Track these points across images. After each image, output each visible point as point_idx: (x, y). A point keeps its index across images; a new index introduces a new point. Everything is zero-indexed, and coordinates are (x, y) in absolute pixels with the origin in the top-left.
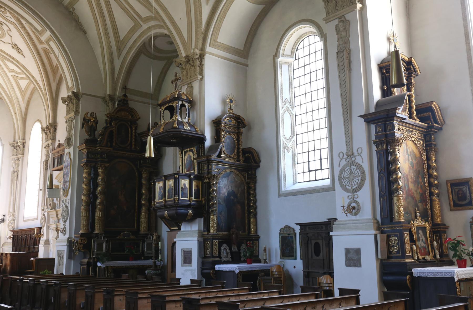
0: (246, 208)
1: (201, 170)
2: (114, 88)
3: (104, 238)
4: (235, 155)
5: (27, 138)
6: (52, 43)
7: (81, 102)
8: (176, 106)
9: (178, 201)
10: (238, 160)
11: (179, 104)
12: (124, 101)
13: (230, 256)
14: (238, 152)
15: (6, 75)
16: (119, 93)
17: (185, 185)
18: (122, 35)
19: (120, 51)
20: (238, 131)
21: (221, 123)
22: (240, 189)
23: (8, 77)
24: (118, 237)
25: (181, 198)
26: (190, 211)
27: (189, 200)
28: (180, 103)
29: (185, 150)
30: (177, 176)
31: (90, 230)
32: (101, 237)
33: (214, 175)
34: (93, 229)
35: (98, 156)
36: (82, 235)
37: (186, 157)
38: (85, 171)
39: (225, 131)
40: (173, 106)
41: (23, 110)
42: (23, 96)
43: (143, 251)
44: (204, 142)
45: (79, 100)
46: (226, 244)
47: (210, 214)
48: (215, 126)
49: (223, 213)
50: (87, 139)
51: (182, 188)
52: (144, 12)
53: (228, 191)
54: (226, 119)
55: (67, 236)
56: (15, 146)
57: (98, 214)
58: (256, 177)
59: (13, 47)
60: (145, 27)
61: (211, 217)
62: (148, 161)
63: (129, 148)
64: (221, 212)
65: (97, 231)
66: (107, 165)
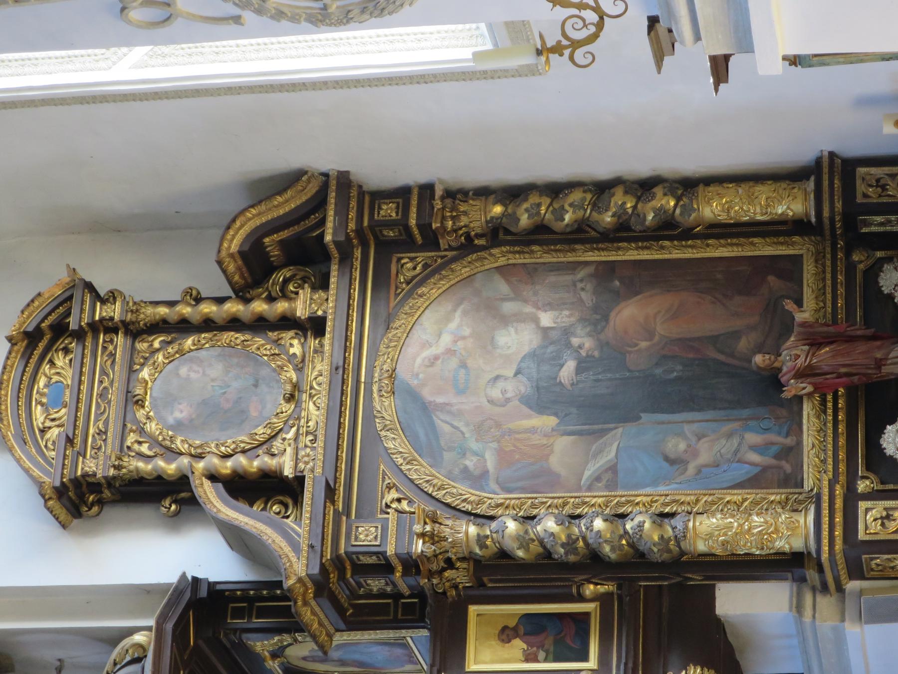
0: (633, 254)
14: (260, 325)
20: (115, 330)
21: (76, 482)
22: (509, 307)
33: (422, 535)
39: (123, 440)
44: (211, 585)
46: (881, 431)
47: (683, 553)
48: (95, 509)
49: (677, 446)
53: (526, 410)
54: (43, 431)
58: (427, 189)
61: (701, 547)
64: (667, 459)
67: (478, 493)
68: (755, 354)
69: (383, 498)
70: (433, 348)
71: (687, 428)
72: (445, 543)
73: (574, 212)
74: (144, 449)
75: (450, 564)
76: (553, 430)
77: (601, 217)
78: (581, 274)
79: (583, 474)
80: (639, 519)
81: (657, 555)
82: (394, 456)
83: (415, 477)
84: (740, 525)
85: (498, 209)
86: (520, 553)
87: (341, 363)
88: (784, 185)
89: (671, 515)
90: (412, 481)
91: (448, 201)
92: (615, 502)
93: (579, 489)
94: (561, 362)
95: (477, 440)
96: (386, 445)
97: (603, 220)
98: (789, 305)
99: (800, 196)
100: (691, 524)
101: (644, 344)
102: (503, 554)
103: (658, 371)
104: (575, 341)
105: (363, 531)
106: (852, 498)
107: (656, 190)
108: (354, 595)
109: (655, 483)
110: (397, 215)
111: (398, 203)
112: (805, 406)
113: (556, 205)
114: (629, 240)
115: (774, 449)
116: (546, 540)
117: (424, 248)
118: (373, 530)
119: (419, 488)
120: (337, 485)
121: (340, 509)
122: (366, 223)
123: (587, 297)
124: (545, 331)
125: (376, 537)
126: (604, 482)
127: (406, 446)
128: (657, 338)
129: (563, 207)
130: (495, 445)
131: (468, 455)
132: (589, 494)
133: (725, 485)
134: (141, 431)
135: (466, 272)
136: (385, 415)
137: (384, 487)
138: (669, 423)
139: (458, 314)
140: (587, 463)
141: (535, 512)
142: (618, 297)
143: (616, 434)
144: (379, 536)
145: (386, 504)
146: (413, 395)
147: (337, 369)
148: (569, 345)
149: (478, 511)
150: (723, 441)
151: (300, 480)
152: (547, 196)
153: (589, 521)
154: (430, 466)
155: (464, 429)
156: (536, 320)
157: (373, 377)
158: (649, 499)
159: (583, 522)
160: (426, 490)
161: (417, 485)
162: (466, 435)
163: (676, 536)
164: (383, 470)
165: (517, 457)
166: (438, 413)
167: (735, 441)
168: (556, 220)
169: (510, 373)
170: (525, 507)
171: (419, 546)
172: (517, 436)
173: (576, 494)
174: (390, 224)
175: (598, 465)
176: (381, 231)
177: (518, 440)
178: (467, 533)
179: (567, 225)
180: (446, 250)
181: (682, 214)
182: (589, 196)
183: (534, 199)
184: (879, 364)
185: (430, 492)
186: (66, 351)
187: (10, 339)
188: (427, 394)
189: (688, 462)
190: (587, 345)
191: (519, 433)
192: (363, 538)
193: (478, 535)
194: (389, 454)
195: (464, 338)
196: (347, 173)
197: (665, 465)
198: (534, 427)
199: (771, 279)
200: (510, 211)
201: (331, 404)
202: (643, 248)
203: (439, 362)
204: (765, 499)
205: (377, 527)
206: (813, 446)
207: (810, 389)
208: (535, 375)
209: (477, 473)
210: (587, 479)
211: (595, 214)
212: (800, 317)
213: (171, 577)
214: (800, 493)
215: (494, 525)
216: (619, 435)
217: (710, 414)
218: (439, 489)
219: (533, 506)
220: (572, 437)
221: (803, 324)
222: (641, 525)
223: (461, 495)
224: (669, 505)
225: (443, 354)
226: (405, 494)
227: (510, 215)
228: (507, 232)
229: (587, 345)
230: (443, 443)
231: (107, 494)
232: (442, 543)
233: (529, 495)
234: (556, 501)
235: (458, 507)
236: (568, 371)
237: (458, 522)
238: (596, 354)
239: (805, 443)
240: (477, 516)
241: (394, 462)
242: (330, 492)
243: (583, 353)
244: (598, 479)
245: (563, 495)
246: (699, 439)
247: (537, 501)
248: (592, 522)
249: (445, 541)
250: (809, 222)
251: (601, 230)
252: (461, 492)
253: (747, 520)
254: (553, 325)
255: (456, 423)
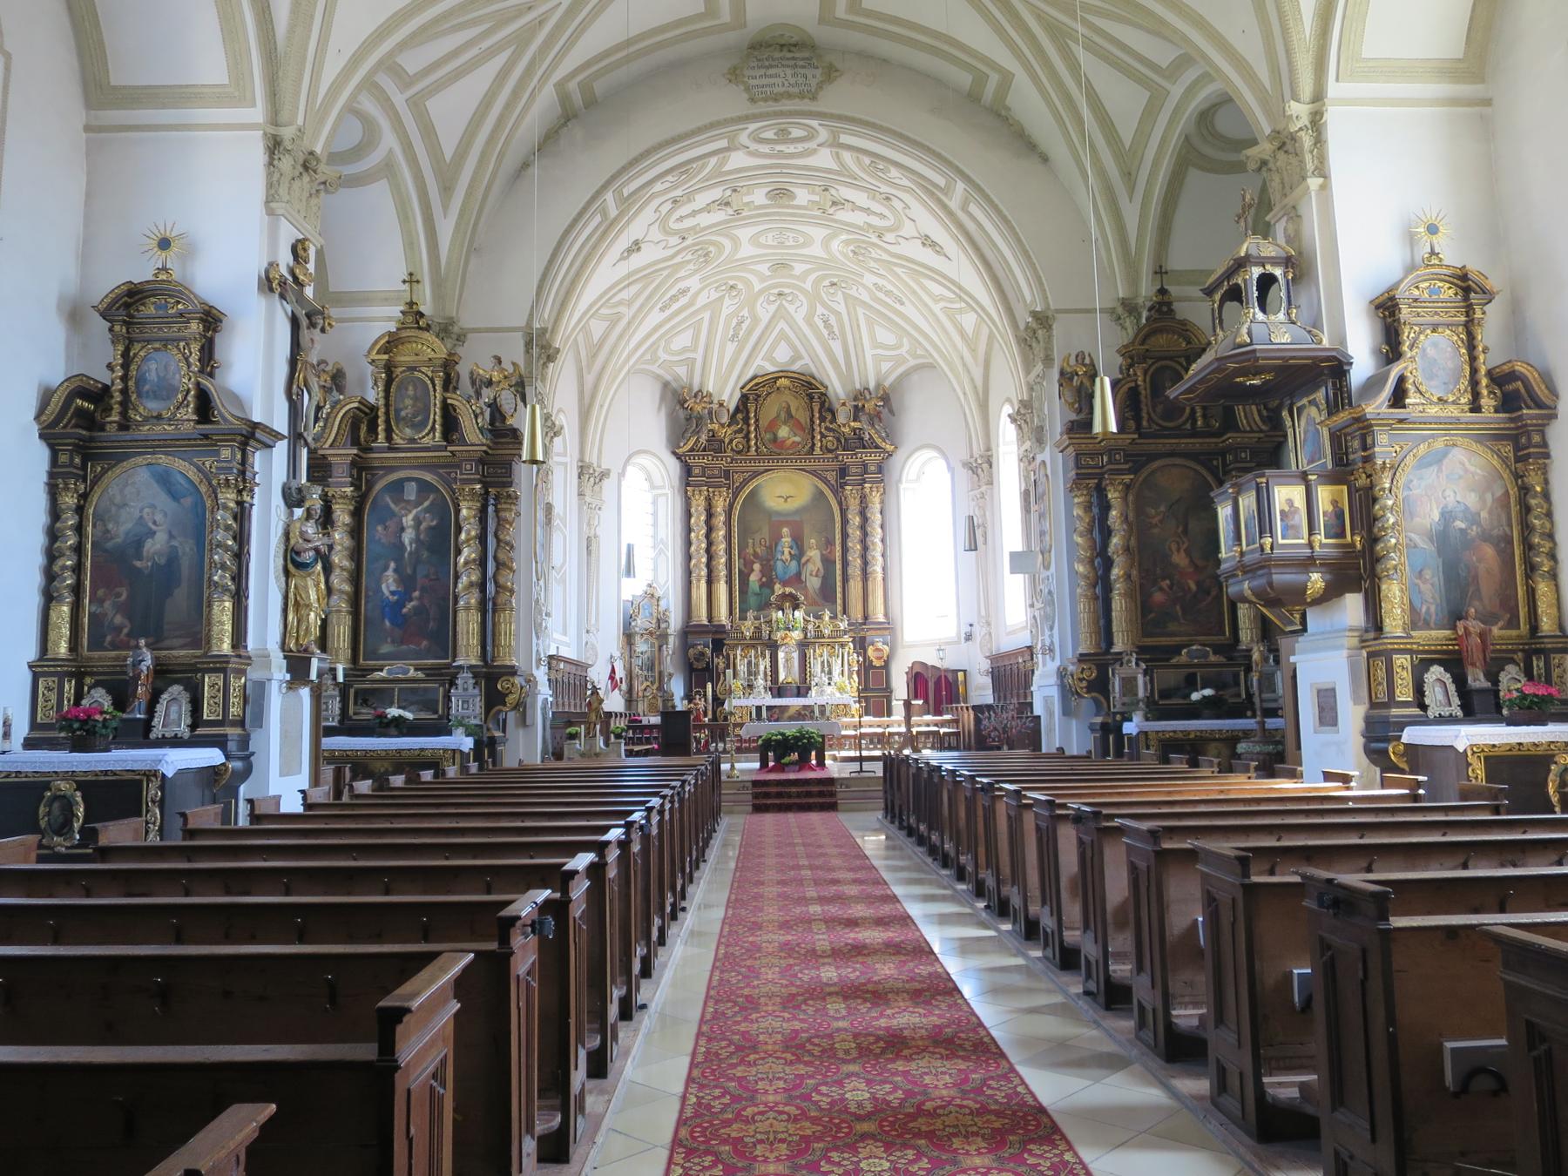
0: (1517, 552)
1: (1347, 454)
2: (1133, 279)
3: (1137, 664)
4: (1462, 395)
5: (993, 446)
6: (973, 208)
7: (1055, 332)
8: (1245, 281)
9: (1272, 549)
10: (1475, 408)
11: (1255, 276)
12: (1163, 307)
13: (1456, 701)
14: (1474, 383)
15: (931, 310)
16: (1146, 290)
17: (1290, 502)
18: (1127, 135)
19: (1129, 177)
20: (1467, 316)
21: (1397, 304)
22: (1489, 497)
23: (934, 315)
24: (1174, 661)
25: (1281, 541)
26: (1315, 576)
27: (1310, 545)
28: (1256, 271)
29: (1299, 404)
30: (1264, 480)
31: (1103, 645)
32: (1129, 661)
33: (1384, 463)
34: (1110, 643)
35: (1105, 459)
36: (1083, 658)
37: (1303, 422)
38: (1076, 500)
40: (1237, 285)
41: (979, 383)
42: (973, 351)
43: (1250, 696)
45: (1049, 328)
46: (1440, 665)
49: (1428, 574)
50: (1072, 422)
51: (1282, 512)
52: (1163, 55)
54: (1417, 287)
55: (1057, 663)
56: (973, 468)
57: (1118, 603)
58: (1547, 456)
59: (924, 244)
60: (1177, 91)
61: (1384, 587)
62: (1243, 455)
63: (1188, 426)
65: (1117, 648)
66: (1127, 478)
71: (1436, 579)
74: (1412, 335)
75: (1369, 476)
78: (1507, 529)
81: (1379, 568)
85: (1538, 489)
86: (1377, 507)
98: (1501, 624)
102: (1375, 500)
106: (1410, 652)
108: (1346, 435)
117: (1515, 455)
123: (1495, 532)
134: (1420, 333)
135: (1505, 476)
142: (1496, 546)
146: (1445, 454)
151: (1404, 407)
169: (1459, 499)
171: (1379, 462)
174: (1529, 439)
183: (1545, 506)
184: (1473, 665)
186: (1456, 294)
187: (1464, 267)
188: (1445, 462)
213: (1350, 352)
228: (1525, 494)
231: (1389, 320)
236: (1460, 524)
242: (1401, 421)
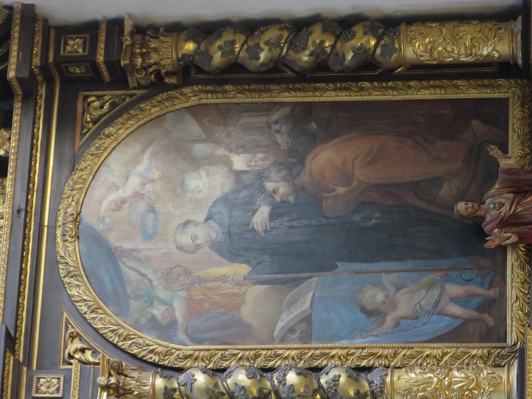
64: (364, 310)
67: (165, 344)
68: (457, 201)
69: (65, 347)
70: (121, 191)
71: (386, 279)
72: (131, 396)
73: (270, 50)
76: (245, 278)
77: (298, 56)
79: (275, 325)
80: (334, 373)
82: (78, 304)
83: (99, 326)
84: (440, 381)
85: (190, 46)
87: (23, 206)
88: (489, 25)
89: (368, 369)
90: (96, 330)
91: (138, 37)
92: (309, 354)
93: (272, 340)
94: (254, 207)
95: (165, 289)
96: (69, 292)
97: (300, 59)
98: (494, 151)
99: (507, 37)
100: (388, 379)
101: (341, 190)
103: (356, 218)
104: (269, 186)
105: (45, 383)
107: (355, 28)
109: (351, 335)
110: (84, 51)
111: (85, 39)
112: (509, 257)
113: (251, 43)
114: (327, 80)
115: (476, 301)
116: (236, 394)
117: (111, 86)
118: (55, 381)
119: (104, 338)
120: (18, 334)
121: (21, 359)
122: (51, 60)
123: (282, 140)
124: (238, 174)
125: (58, 389)
126: (298, 334)
127: (91, 293)
128: (355, 183)
129: (258, 45)
130: (184, 294)
131: (156, 303)
132: (282, 346)
133: (424, 338)
135: (155, 111)
136: (69, 260)
137: (67, 337)
138: (367, 272)
139: (147, 155)
140: (280, 313)
141: (225, 364)
143: (311, 283)
144: (61, 388)
145: (69, 354)
147: (19, 211)
148: (262, 190)
149: (166, 363)
150: (423, 292)
152: (241, 33)
153: (282, 375)
154: (116, 315)
155: (151, 276)
156: (228, 164)
157: (56, 221)
158: (345, 352)
159: (276, 375)
160: (111, 340)
161: (101, 335)
162: (155, 283)
163: (372, 392)
164: (66, 319)
165: (207, 306)
166: (125, 260)
167: (436, 292)
168: (251, 58)
169: (201, 218)
170: (215, 359)
172: (208, 285)
173: (268, 346)
174: (77, 60)
175: (291, 316)
176: (67, 68)
177: (209, 288)
178: (153, 386)
179: (262, 64)
180: (134, 88)
181: (382, 54)
182: (285, 34)
183: (228, 36)
185: (115, 342)
189: (386, 314)
190: (282, 190)
191: (209, 281)
192: (45, 390)
193: (166, 388)
194: (73, 302)
195: (153, 181)
196: (32, 6)
197: (362, 316)
198: (225, 275)
199: (475, 123)
200: (202, 48)
201: (12, 248)
202: (341, 89)
203: (127, 205)
204: (466, 353)
205: (59, 379)
206: (517, 298)
207: (514, 239)
208: (226, 220)
209: (165, 322)
210: (280, 331)
211: (291, 53)
212: (505, 163)
214: (503, 348)
215: (182, 377)
216: (314, 285)
217: (409, 264)
218: (125, 339)
219: (223, 358)
220: (265, 287)
221: (509, 171)
222: (336, 380)
223: (148, 345)
224: (365, 359)
225: (130, 197)
226: (89, 344)
227: (202, 52)
228: (199, 70)
229: (282, 190)
230: (129, 292)
232: (128, 396)
233: (219, 347)
234: (247, 353)
235: (145, 358)
237: (144, 375)
238: (291, 199)
239: (509, 295)
240: (164, 368)
241: (78, 310)
243: (278, 198)
244: (292, 330)
245: (255, 346)
246: (398, 290)
247: (227, 353)
248: (285, 375)
249: (130, 394)
250: (516, 64)
251: (298, 69)
252: (147, 342)
253: (447, 375)
254: (246, 169)
255: (143, 270)
